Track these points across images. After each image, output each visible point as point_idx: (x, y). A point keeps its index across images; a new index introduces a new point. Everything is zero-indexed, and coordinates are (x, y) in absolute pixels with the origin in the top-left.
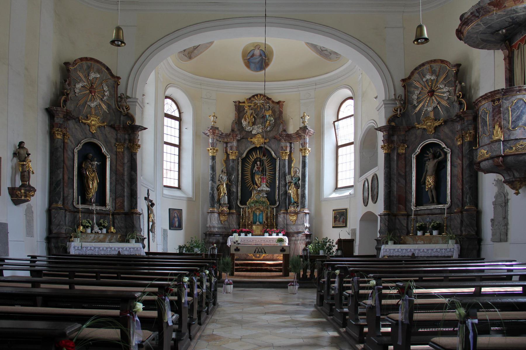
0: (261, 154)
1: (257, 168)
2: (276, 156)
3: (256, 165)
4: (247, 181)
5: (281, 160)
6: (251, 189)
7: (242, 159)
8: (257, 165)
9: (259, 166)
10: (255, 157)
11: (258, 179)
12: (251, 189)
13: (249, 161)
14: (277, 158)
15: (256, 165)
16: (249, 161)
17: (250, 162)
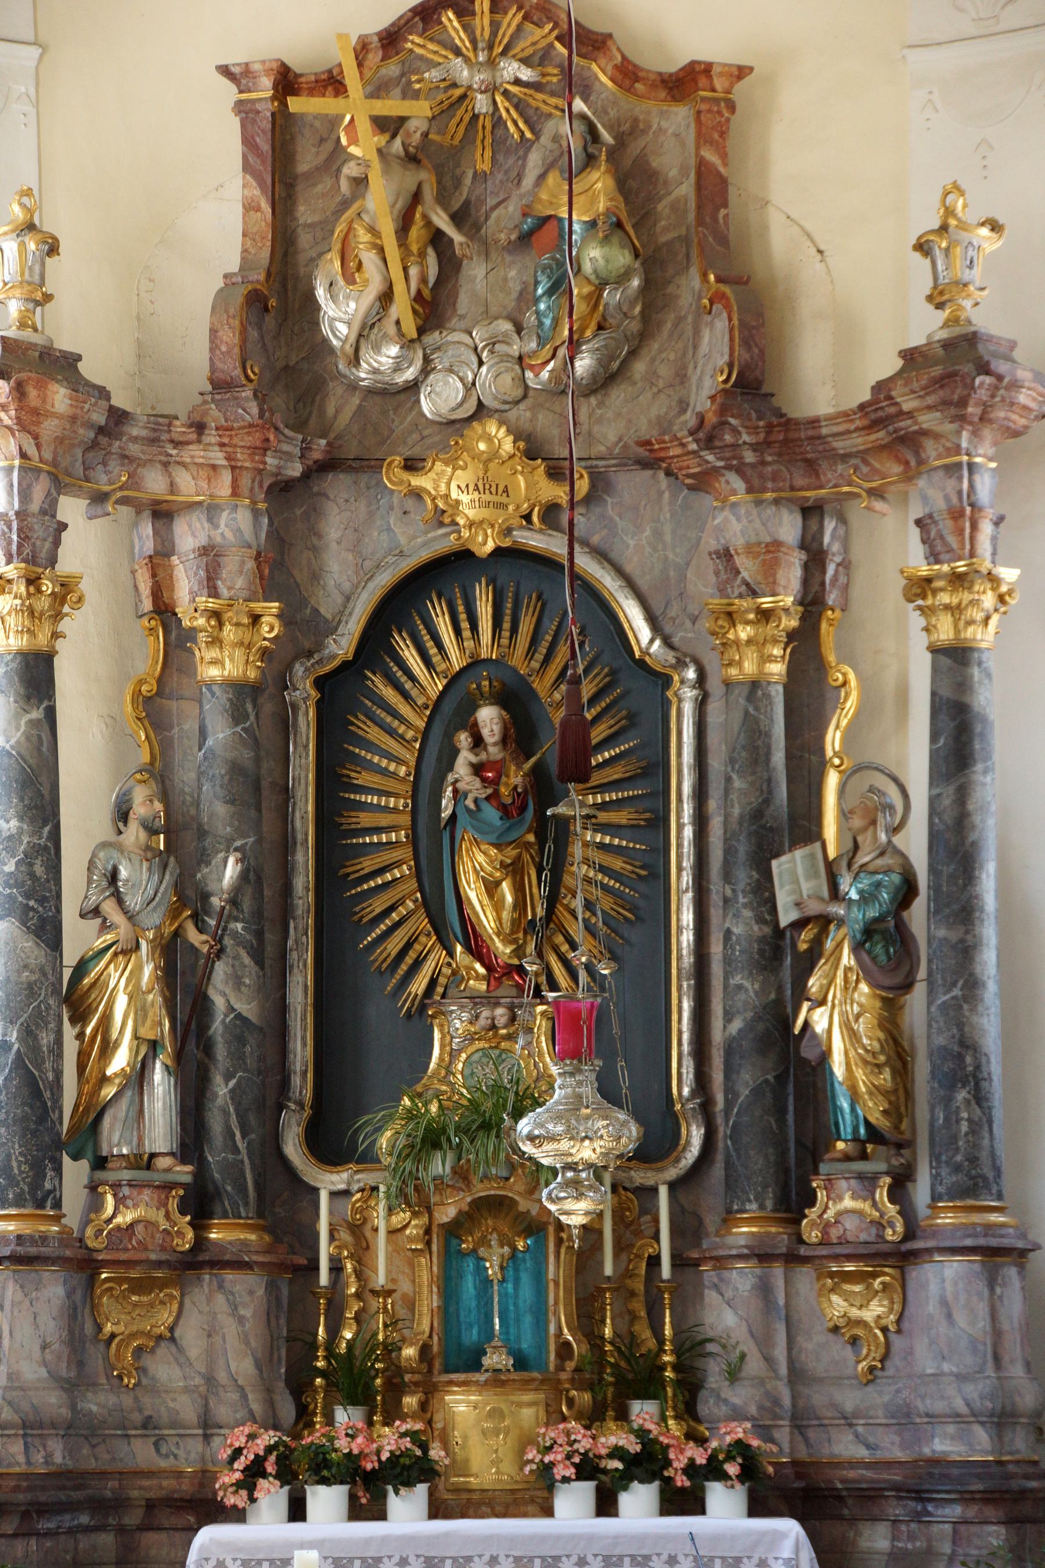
0: (514, 630)
1: (478, 769)
2: (667, 643)
3: (463, 739)
4: (378, 905)
5: (714, 684)
6: (419, 985)
7: (319, 683)
8: (478, 742)
9: (494, 752)
10: (457, 661)
11: (491, 888)
12: (419, 985)
13: (389, 693)
14: (680, 664)
15: (463, 739)
16: (389, 693)
17: (404, 709)
